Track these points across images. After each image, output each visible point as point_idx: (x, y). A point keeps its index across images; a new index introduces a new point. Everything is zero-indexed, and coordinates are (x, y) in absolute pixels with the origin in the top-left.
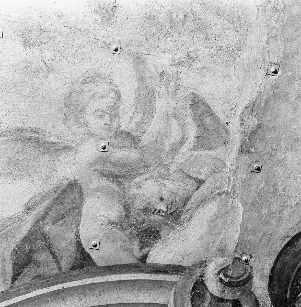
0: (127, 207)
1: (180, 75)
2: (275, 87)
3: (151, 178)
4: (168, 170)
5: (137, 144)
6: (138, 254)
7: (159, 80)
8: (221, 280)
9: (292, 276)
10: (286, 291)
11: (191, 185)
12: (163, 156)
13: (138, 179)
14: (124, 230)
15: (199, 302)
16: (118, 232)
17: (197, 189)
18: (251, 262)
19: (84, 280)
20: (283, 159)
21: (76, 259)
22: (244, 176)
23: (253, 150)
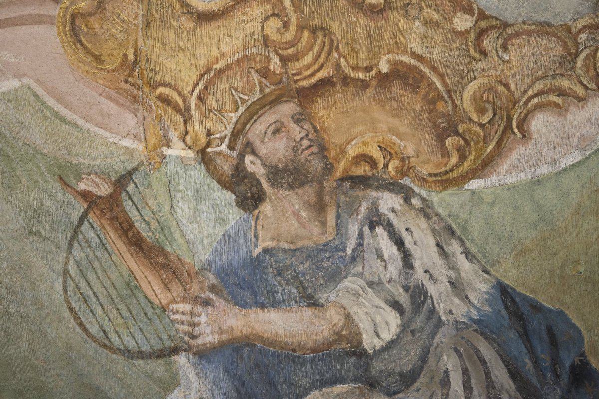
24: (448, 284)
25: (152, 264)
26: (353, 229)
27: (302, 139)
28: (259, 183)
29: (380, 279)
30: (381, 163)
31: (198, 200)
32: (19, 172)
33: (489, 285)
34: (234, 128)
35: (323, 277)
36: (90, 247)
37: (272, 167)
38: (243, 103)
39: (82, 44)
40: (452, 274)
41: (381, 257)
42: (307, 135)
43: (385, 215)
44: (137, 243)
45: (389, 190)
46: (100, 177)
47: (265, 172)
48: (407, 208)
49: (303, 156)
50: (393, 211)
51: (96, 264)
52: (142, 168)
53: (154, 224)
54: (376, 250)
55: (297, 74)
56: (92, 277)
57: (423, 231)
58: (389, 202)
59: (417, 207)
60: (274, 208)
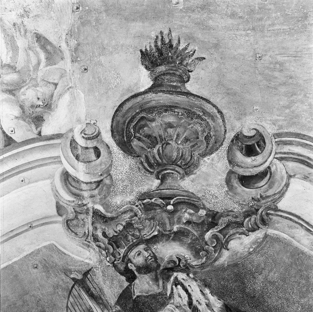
0: (22, 107)
1: (25, 23)
2: (80, 18)
3: (29, 88)
4: (37, 81)
5: (15, 69)
6: (36, 132)
7: (14, 29)
8: (83, 137)
9: (124, 128)
10: (123, 137)
11: (52, 87)
12: (31, 74)
13: (22, 90)
14: (24, 120)
15: (76, 152)
16: (22, 122)
17: (56, 89)
18: (98, 124)
19: (13, 151)
20: (99, 61)
21: (5, 141)
22: (79, 76)
23: (79, 59)
24: (206, 305)
25: (97, 303)
26: (169, 287)
27: (148, 256)
28: (134, 273)
29: (180, 305)
30: (178, 263)
31: (112, 280)
32: (51, 272)
33: (221, 305)
34: (124, 255)
35: (159, 305)
36: (75, 297)
37: (138, 267)
38: (126, 246)
39: (70, 229)
40: (207, 301)
41: (180, 296)
42: (150, 255)
43: (180, 281)
44: (92, 296)
45: (181, 272)
46: (78, 273)
47: (136, 269)
48: (188, 278)
49: (149, 262)
50: (183, 279)
51: (78, 303)
52: (92, 269)
53: (98, 289)
54: (178, 294)
55: (145, 235)
56: (76, 308)
57: (195, 286)
58: (181, 276)
59: (192, 277)
60: (139, 280)
